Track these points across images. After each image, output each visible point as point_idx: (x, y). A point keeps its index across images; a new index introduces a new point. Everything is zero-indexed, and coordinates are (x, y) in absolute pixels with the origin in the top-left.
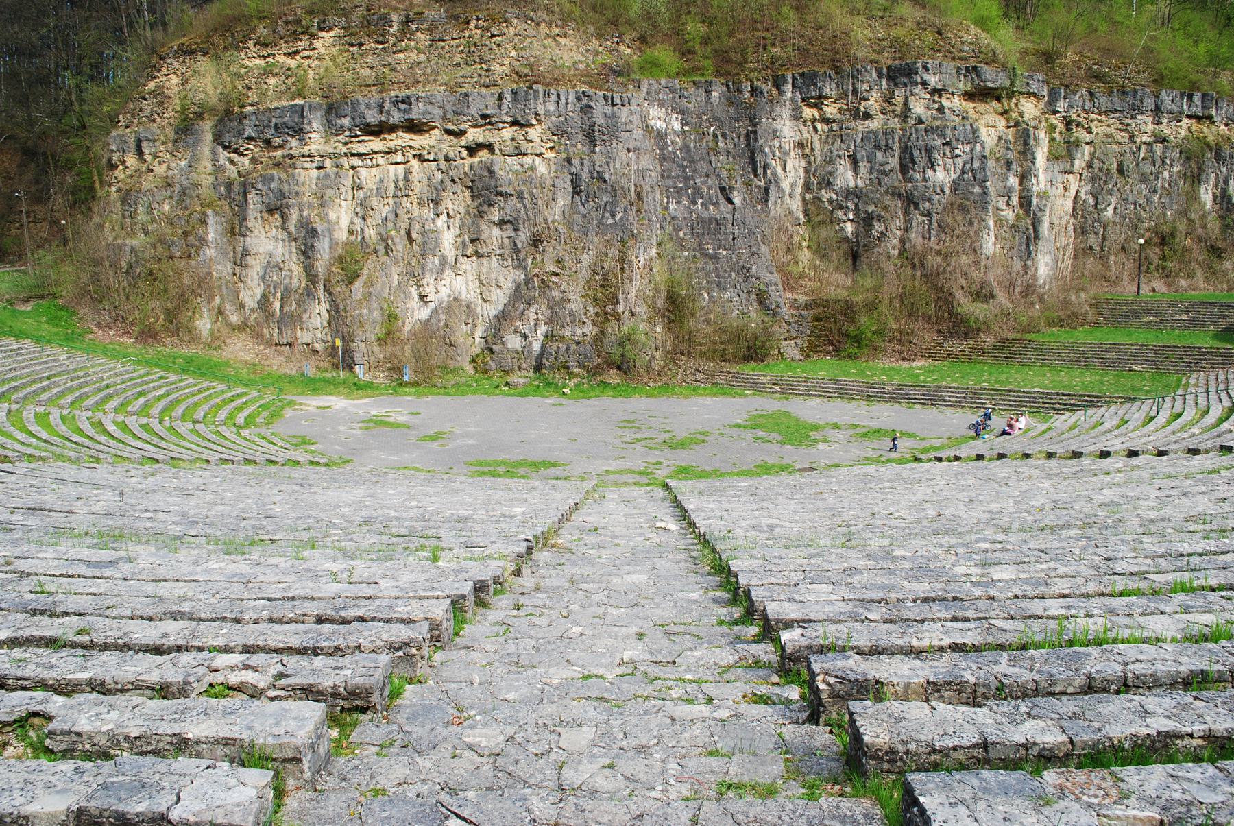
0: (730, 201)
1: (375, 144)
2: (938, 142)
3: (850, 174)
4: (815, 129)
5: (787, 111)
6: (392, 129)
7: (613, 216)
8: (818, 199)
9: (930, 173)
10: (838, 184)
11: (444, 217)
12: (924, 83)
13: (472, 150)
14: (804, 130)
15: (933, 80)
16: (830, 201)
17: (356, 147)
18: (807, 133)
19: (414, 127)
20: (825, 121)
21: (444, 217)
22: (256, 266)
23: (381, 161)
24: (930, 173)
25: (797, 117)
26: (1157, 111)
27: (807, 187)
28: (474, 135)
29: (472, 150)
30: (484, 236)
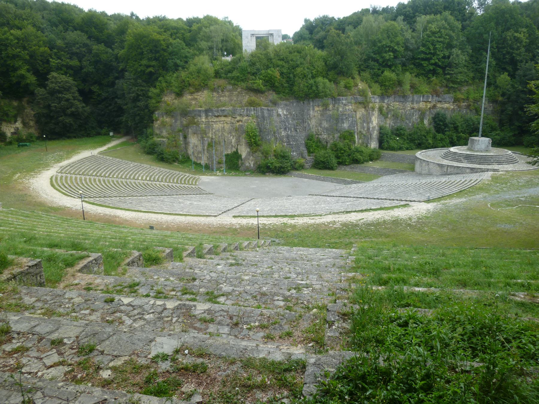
0: (296, 131)
1: (216, 119)
2: (344, 118)
3: (325, 124)
5: (311, 108)
6: (221, 116)
8: (318, 129)
10: (323, 126)
13: (238, 121)
15: (344, 102)
17: (213, 120)
19: (225, 116)
22: (191, 145)
25: (313, 110)
27: (316, 126)
28: (238, 118)
29: (238, 121)
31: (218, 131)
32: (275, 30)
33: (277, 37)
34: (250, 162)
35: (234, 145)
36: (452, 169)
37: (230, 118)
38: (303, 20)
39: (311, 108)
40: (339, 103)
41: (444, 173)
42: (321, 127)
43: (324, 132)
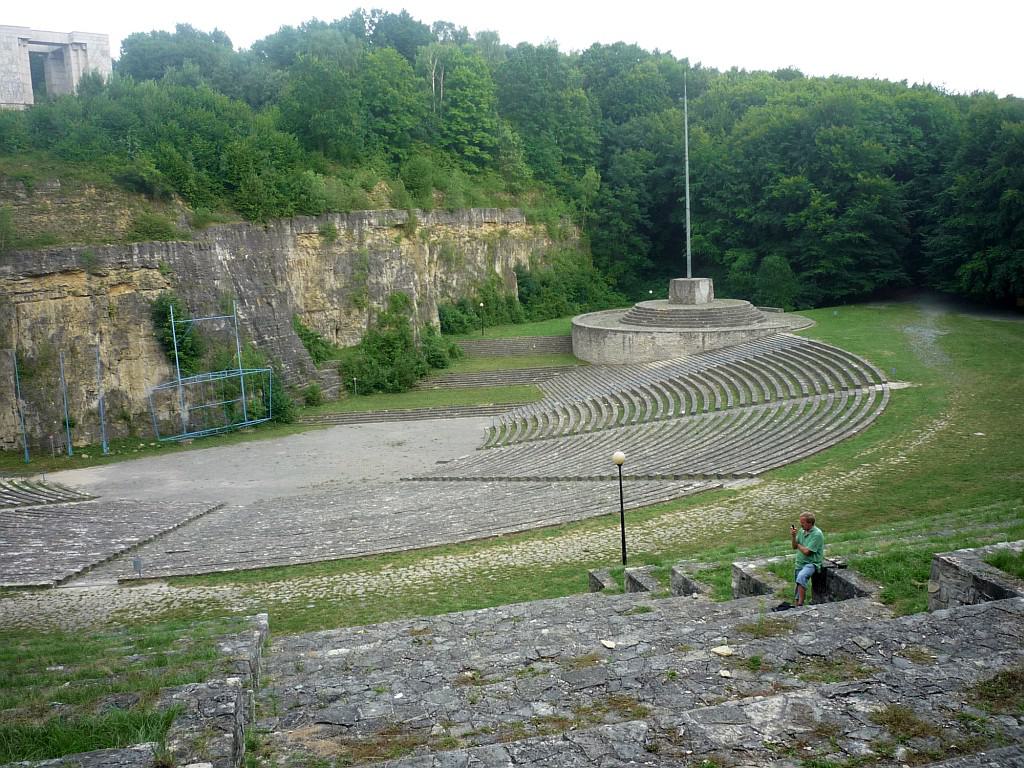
1: (35, 285)
3: (332, 279)
4: (308, 253)
5: (290, 241)
7: (219, 325)
9: (380, 279)
10: (327, 287)
11: (98, 335)
12: (370, 224)
14: (301, 254)
16: (323, 298)
17: (19, 289)
18: (303, 256)
19: (66, 272)
20: (315, 248)
21: (98, 335)
23: (41, 297)
24: (380, 279)
26: (470, 223)
30: (132, 345)
31: (44, 321)
32: (91, 35)
33: (98, 54)
34: (177, 406)
35: (105, 361)
36: (715, 339)
37: (84, 276)
38: (355, 9)
39: (290, 241)
40: (361, 224)
41: (697, 351)
42: (322, 288)
43: (332, 302)
